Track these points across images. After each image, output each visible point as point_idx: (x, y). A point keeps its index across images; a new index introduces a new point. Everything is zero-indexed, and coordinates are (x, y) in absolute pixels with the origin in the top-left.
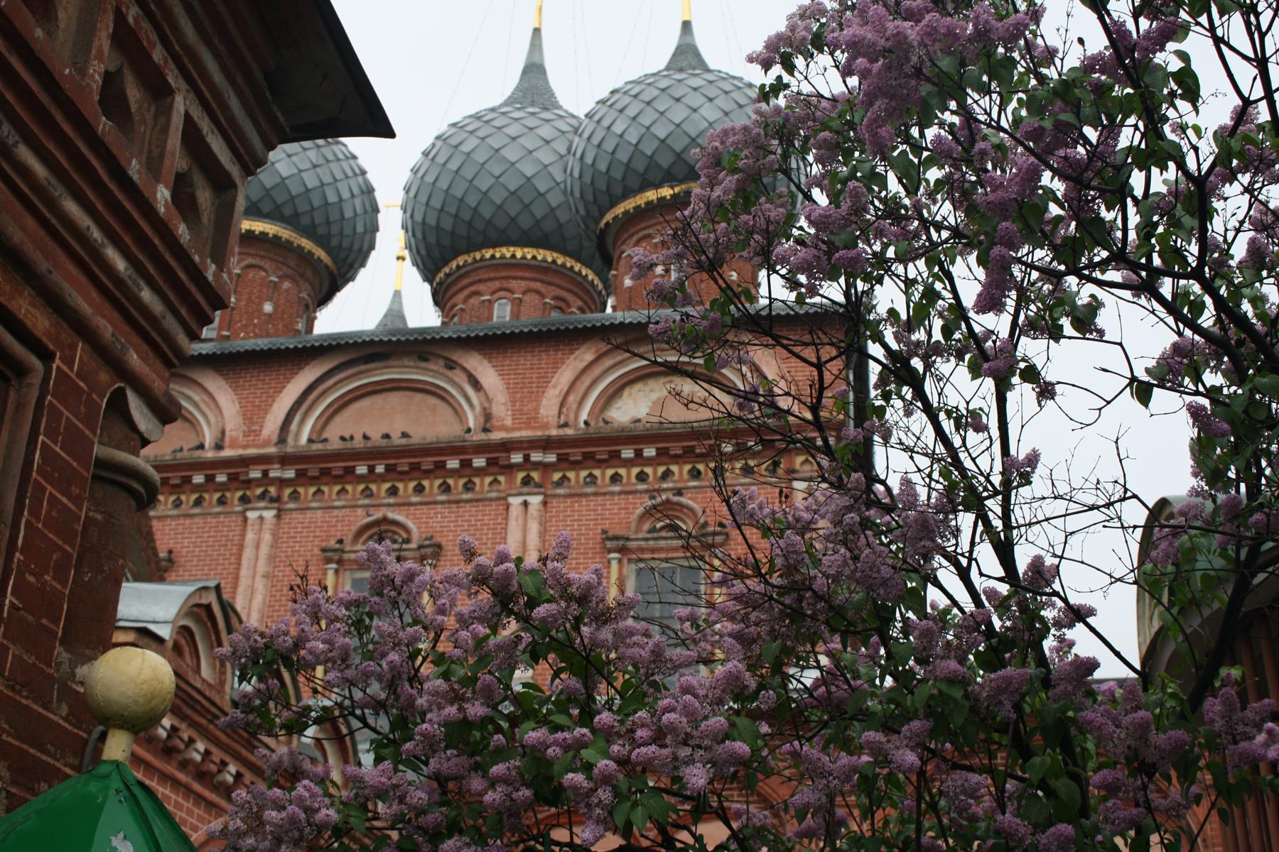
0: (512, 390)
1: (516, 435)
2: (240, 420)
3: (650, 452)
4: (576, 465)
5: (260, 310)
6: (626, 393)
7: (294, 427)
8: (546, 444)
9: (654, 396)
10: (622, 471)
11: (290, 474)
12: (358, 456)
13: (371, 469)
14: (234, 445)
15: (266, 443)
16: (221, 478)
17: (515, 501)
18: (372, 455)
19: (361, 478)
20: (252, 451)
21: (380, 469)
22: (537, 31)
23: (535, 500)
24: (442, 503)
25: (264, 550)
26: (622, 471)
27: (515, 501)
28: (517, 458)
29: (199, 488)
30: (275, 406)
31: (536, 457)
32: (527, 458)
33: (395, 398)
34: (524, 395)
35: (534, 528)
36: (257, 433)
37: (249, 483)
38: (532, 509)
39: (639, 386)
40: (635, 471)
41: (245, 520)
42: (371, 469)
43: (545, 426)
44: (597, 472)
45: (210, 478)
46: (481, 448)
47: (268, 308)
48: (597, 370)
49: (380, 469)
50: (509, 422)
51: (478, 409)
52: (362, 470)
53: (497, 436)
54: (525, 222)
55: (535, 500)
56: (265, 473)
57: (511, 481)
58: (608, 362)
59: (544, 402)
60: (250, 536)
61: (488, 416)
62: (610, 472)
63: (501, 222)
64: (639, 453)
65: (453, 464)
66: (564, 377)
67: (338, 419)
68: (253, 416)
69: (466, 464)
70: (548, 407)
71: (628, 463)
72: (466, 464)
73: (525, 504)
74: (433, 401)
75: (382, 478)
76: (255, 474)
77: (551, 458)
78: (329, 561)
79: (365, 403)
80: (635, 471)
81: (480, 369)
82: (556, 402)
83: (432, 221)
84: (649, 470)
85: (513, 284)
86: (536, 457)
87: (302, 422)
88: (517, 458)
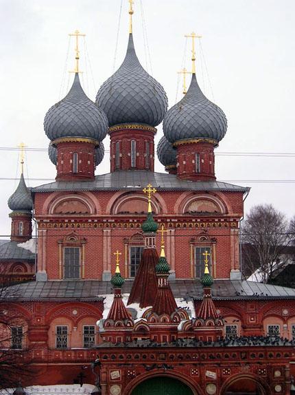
1: (169, 215)
3: (199, 220)
5: (87, 163)
8: (175, 218)
11: (113, 221)
16: (96, 221)
20: (104, 216)
21: (135, 221)
22: (131, 34)
31: (173, 220)
34: (170, 204)
37: (103, 222)
45: (93, 221)
47: (89, 162)
49: (135, 221)
53: (164, 215)
55: (173, 231)
61: (161, 209)
66: (179, 201)
67: (123, 206)
68: (103, 206)
71: (194, 222)
76: (105, 221)
79: (129, 202)
86: (173, 220)
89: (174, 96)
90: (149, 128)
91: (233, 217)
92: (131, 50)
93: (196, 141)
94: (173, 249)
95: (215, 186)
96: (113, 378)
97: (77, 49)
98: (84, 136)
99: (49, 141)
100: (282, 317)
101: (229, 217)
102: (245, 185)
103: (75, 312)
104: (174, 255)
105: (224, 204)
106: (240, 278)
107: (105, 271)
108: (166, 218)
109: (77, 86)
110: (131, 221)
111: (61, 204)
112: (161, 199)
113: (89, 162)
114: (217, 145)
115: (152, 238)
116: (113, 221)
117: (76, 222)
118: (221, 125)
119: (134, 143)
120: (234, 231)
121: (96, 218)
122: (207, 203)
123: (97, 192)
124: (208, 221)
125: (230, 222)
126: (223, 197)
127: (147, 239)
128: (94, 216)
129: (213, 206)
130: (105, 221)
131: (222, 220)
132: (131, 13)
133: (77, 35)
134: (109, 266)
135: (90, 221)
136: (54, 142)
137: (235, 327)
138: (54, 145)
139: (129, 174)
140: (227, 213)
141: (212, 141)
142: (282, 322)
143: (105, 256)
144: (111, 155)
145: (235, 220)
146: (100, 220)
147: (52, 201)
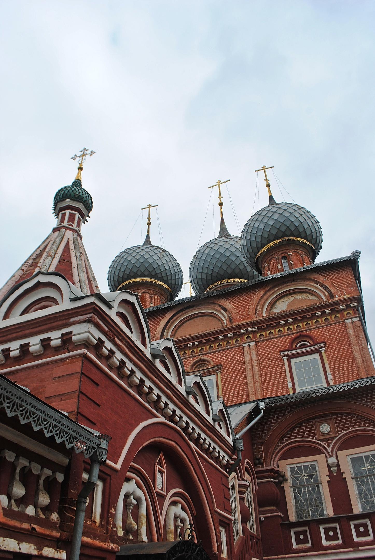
3: (290, 320)
4: (265, 330)
6: (277, 303)
8: (253, 324)
9: (287, 302)
10: (282, 329)
12: (188, 340)
13: (193, 344)
17: (245, 345)
19: (190, 348)
21: (196, 343)
23: (252, 344)
24: (220, 351)
26: (282, 329)
27: (245, 345)
28: (243, 331)
30: (158, 329)
31: (250, 329)
32: (247, 330)
35: (254, 353)
38: (251, 347)
40: (286, 328)
42: (193, 344)
43: (251, 317)
44: (273, 331)
46: (229, 330)
48: (266, 297)
49: (196, 343)
51: (227, 317)
52: (190, 345)
53: (236, 324)
54: (229, 271)
55: (252, 344)
57: (243, 340)
59: (250, 310)
62: (277, 330)
63: (222, 273)
64: (286, 321)
65: (221, 337)
66: (255, 300)
69: (226, 336)
71: (283, 326)
72: (226, 336)
73: (249, 346)
74: (211, 318)
75: (197, 347)
77: (256, 329)
80: (286, 328)
81: (225, 304)
83: (199, 276)
84: (291, 327)
86: (250, 329)
87: (168, 332)
88: (243, 331)
91: (344, 301)
94: (256, 369)
104: (257, 378)
105: (325, 288)
108: (239, 327)
120: (352, 322)
122: (298, 297)
125: (341, 311)
126: (322, 279)
131: (328, 311)
133: (150, 206)
140: (332, 296)
145: (348, 306)
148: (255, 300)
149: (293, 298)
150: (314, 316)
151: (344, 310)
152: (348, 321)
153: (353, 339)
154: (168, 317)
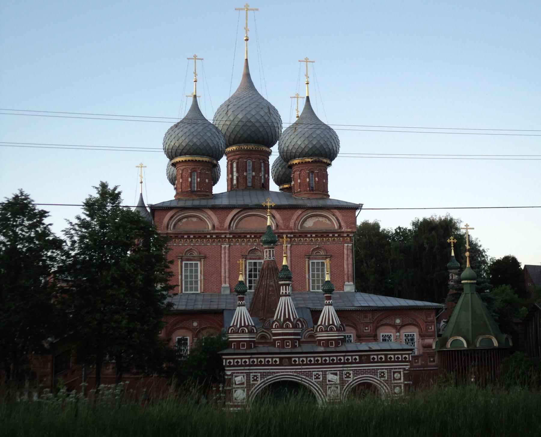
0: (283, 220)
1: (285, 231)
2: (218, 223)
3: (314, 235)
4: (297, 237)
5: (205, 181)
7: (232, 225)
8: (291, 233)
9: (314, 221)
11: (231, 236)
13: (251, 236)
14: (218, 229)
15: (226, 229)
16: (214, 236)
18: (251, 233)
19: (248, 238)
20: (223, 231)
21: (253, 236)
22: (247, 60)
25: (227, 255)
29: (209, 238)
31: (289, 236)
33: (254, 217)
34: (286, 220)
36: (223, 227)
37: (221, 238)
38: (288, 248)
39: (310, 219)
41: (221, 247)
42: (251, 236)
43: (291, 229)
45: (211, 236)
47: (207, 181)
49: (253, 236)
50: (283, 227)
53: (282, 231)
56: (225, 236)
58: (304, 214)
60: (223, 252)
64: (311, 236)
66: (295, 217)
68: (222, 221)
70: (292, 224)
71: (309, 238)
74: (263, 219)
75: (253, 238)
76: (223, 236)
77: (292, 236)
78: (243, 258)
79: (246, 219)
82: (293, 223)
85: (252, 156)
86: (289, 236)
89: (288, 116)
90: (264, 148)
91: (346, 232)
92: (247, 75)
93: (310, 160)
95: (329, 203)
96: (237, 383)
97: (195, 73)
98: (203, 155)
99: (168, 160)
100: (395, 326)
101: (343, 232)
102: (357, 202)
103: (195, 324)
105: (338, 220)
106: (354, 291)
107: (223, 285)
109: (195, 107)
110: (248, 236)
111: (180, 220)
112: (277, 216)
113: (207, 181)
114: (329, 165)
115: (271, 250)
116: (231, 236)
117: (194, 237)
118: (334, 145)
119: (250, 163)
120: (348, 246)
121: (213, 234)
122: (321, 219)
123: (214, 208)
124: (322, 236)
125: (343, 237)
126: (337, 213)
127: (266, 251)
128: (212, 232)
129: (328, 222)
130: (223, 236)
131: (336, 235)
132: (247, 40)
134: (227, 280)
135: (208, 236)
136: (173, 161)
137: (350, 336)
138: (174, 165)
139: (247, 193)
140: (340, 227)
141: (325, 161)
142: (394, 331)
143: (223, 270)
144: (228, 175)
145: (348, 236)
146: (218, 236)
147: (172, 217)
148: (295, 217)
149: (317, 219)
150: (328, 236)
151: (345, 237)
152: (346, 245)
153: (345, 256)
154: (234, 212)
